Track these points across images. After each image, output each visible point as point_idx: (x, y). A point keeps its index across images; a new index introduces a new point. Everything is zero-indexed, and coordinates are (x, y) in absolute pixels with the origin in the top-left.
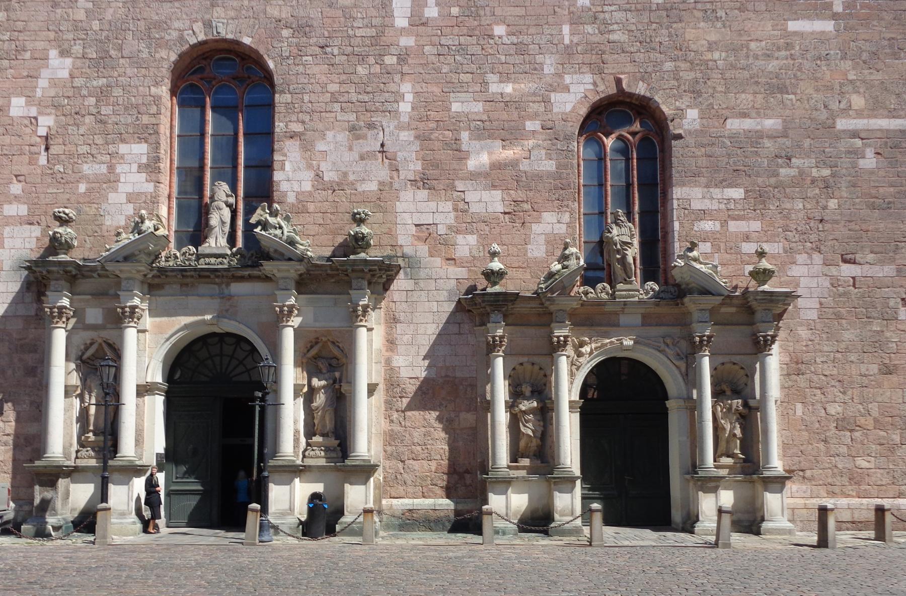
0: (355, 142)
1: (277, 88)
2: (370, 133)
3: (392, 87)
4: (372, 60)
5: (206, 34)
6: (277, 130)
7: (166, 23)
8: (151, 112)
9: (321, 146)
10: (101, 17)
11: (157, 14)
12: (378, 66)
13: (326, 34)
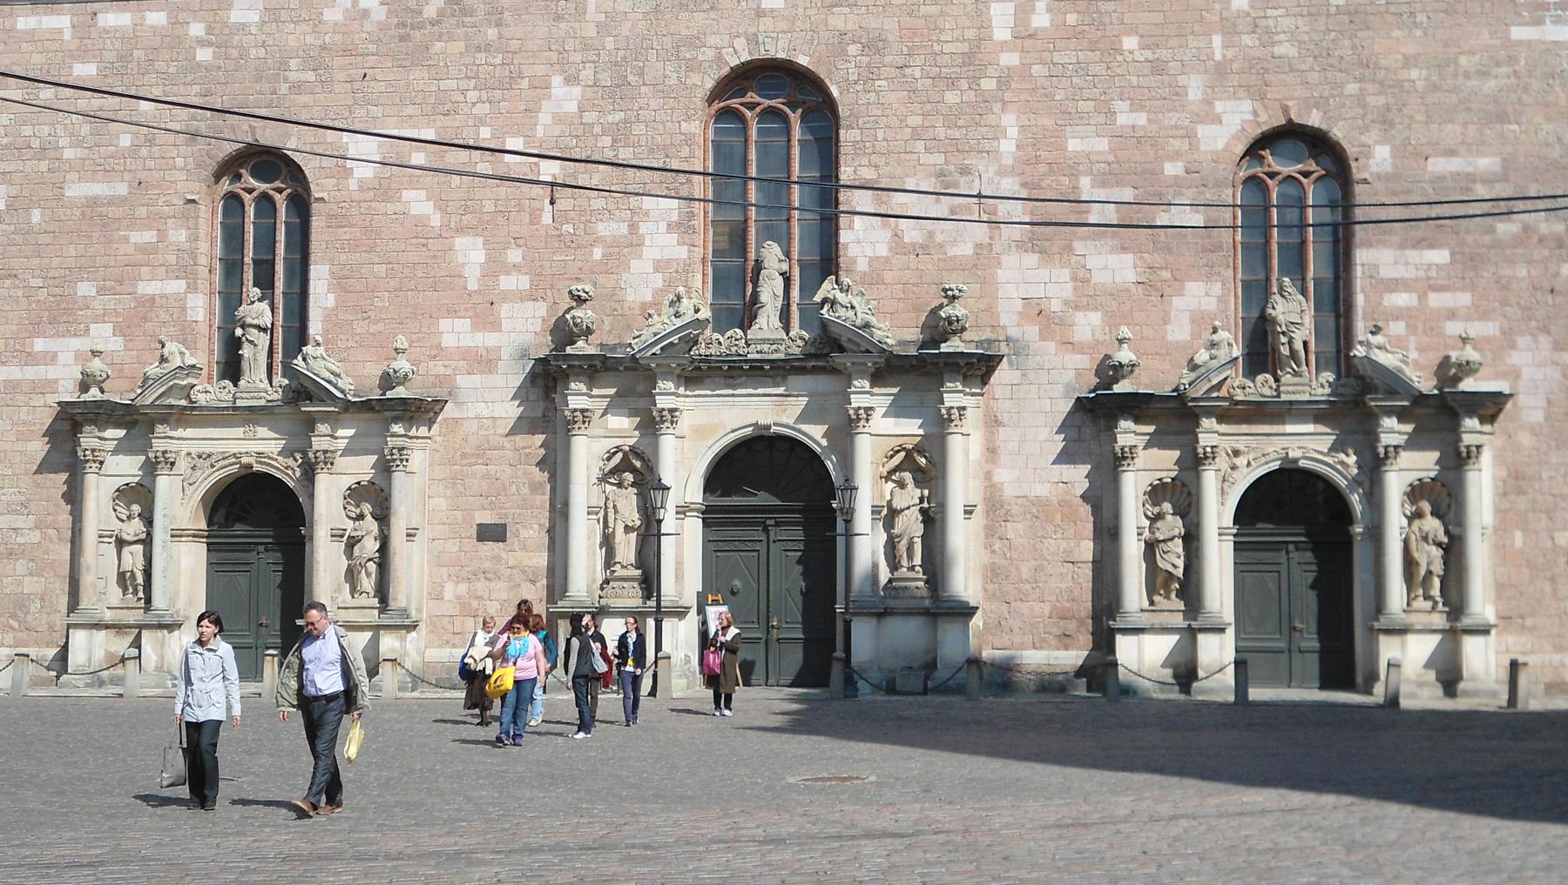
1: (842, 122)
3: (992, 119)
4: (964, 84)
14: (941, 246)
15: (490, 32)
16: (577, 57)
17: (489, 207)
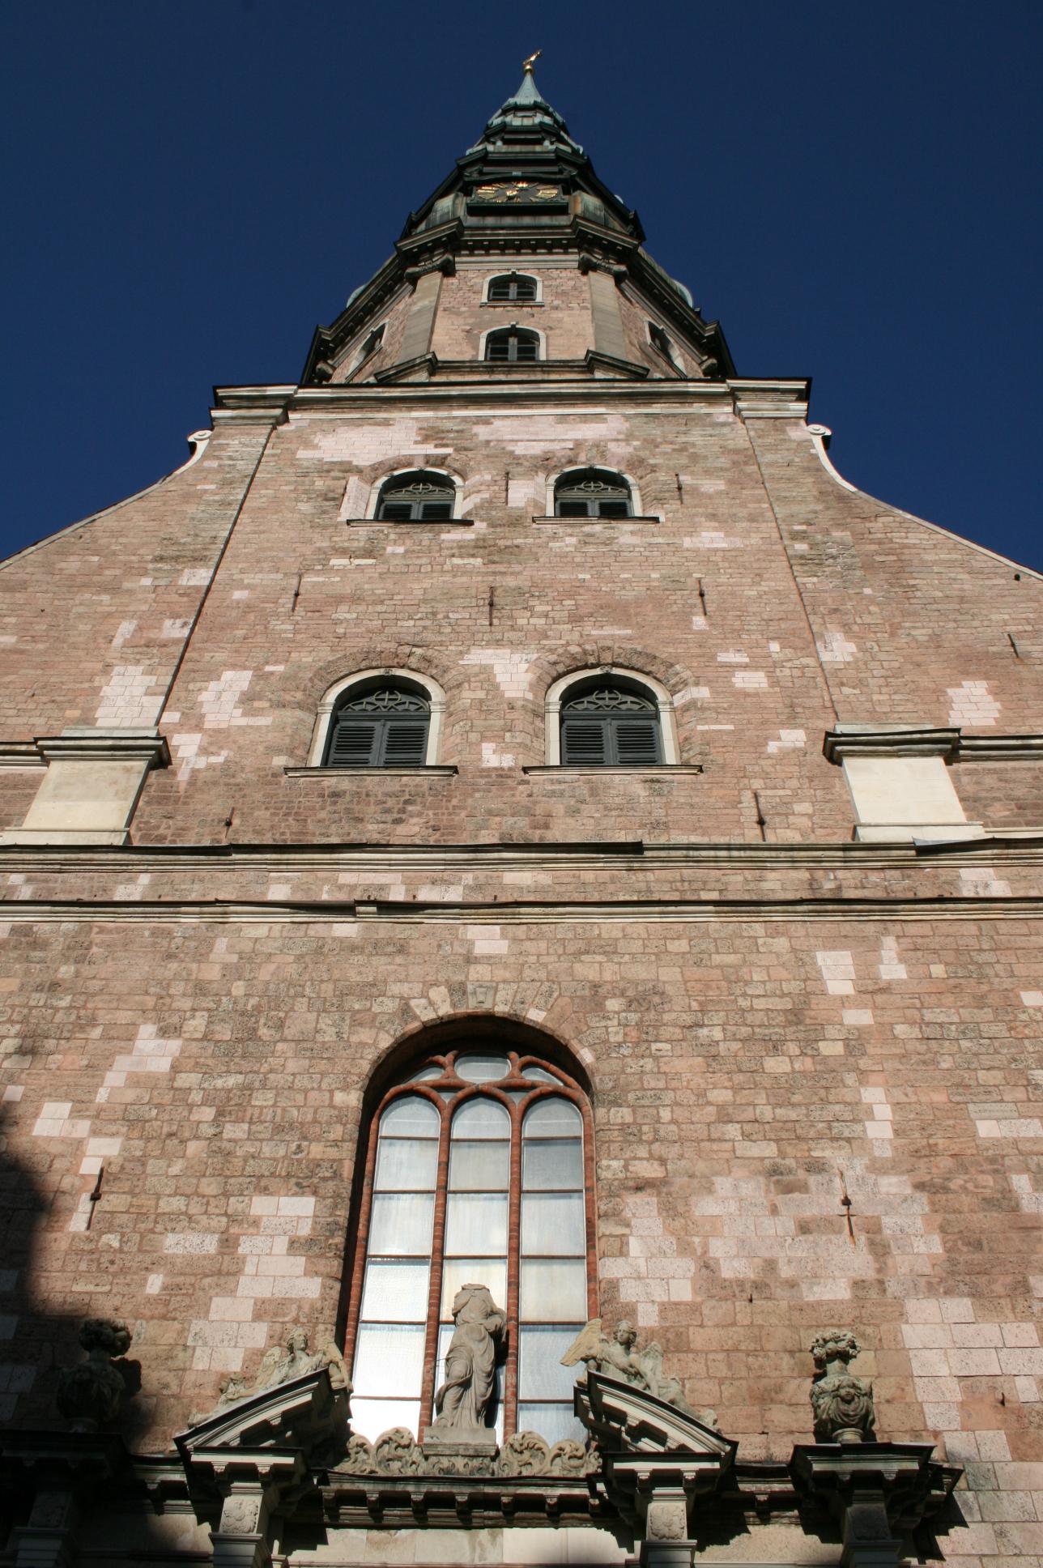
2: (813, 1180)
4: (793, 1048)
5: (454, 1005)
11: (360, 973)
12: (808, 1060)
14: (792, 1284)
15: (63, 969)
16: (186, 1004)
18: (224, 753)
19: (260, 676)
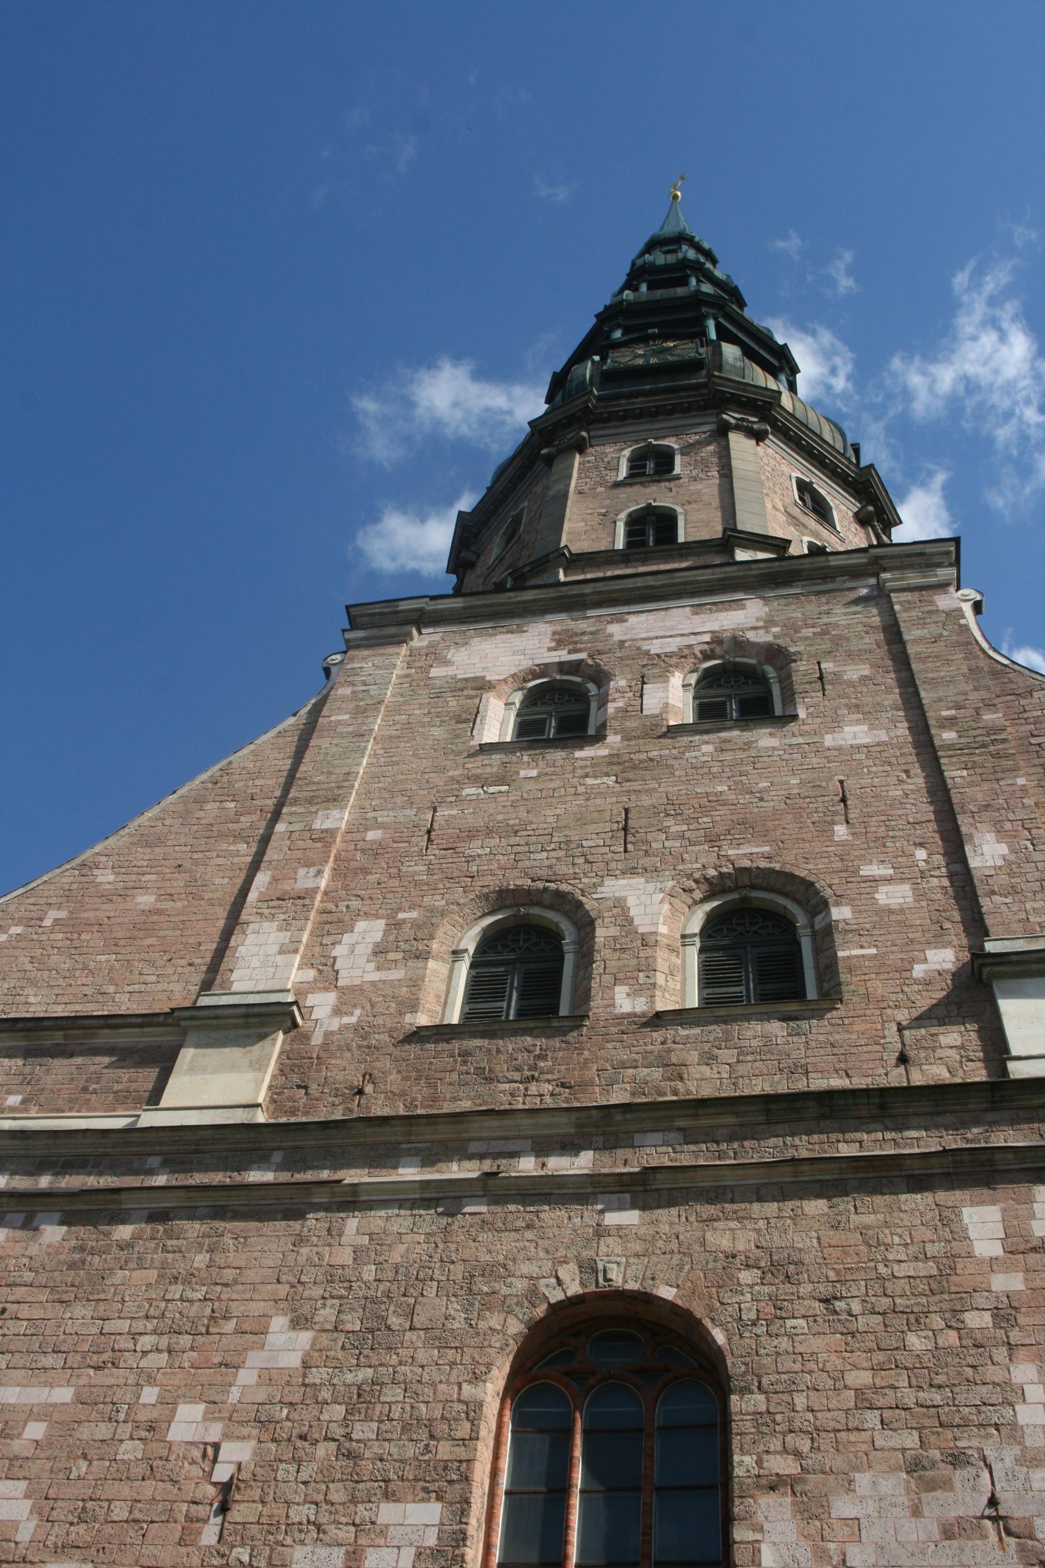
0: (926, 1497)
1: (735, 1383)
2: (959, 1476)
3: (994, 1373)
5: (582, 1284)
6: (738, 1471)
7: (504, 1266)
8: (459, 1435)
9: (843, 1507)
10: (381, 1259)
11: (489, 1251)
12: (953, 1334)
13: (832, 1276)
15: (199, 1257)
17: (120, 1512)
18: (358, 1012)
19: (393, 925)
